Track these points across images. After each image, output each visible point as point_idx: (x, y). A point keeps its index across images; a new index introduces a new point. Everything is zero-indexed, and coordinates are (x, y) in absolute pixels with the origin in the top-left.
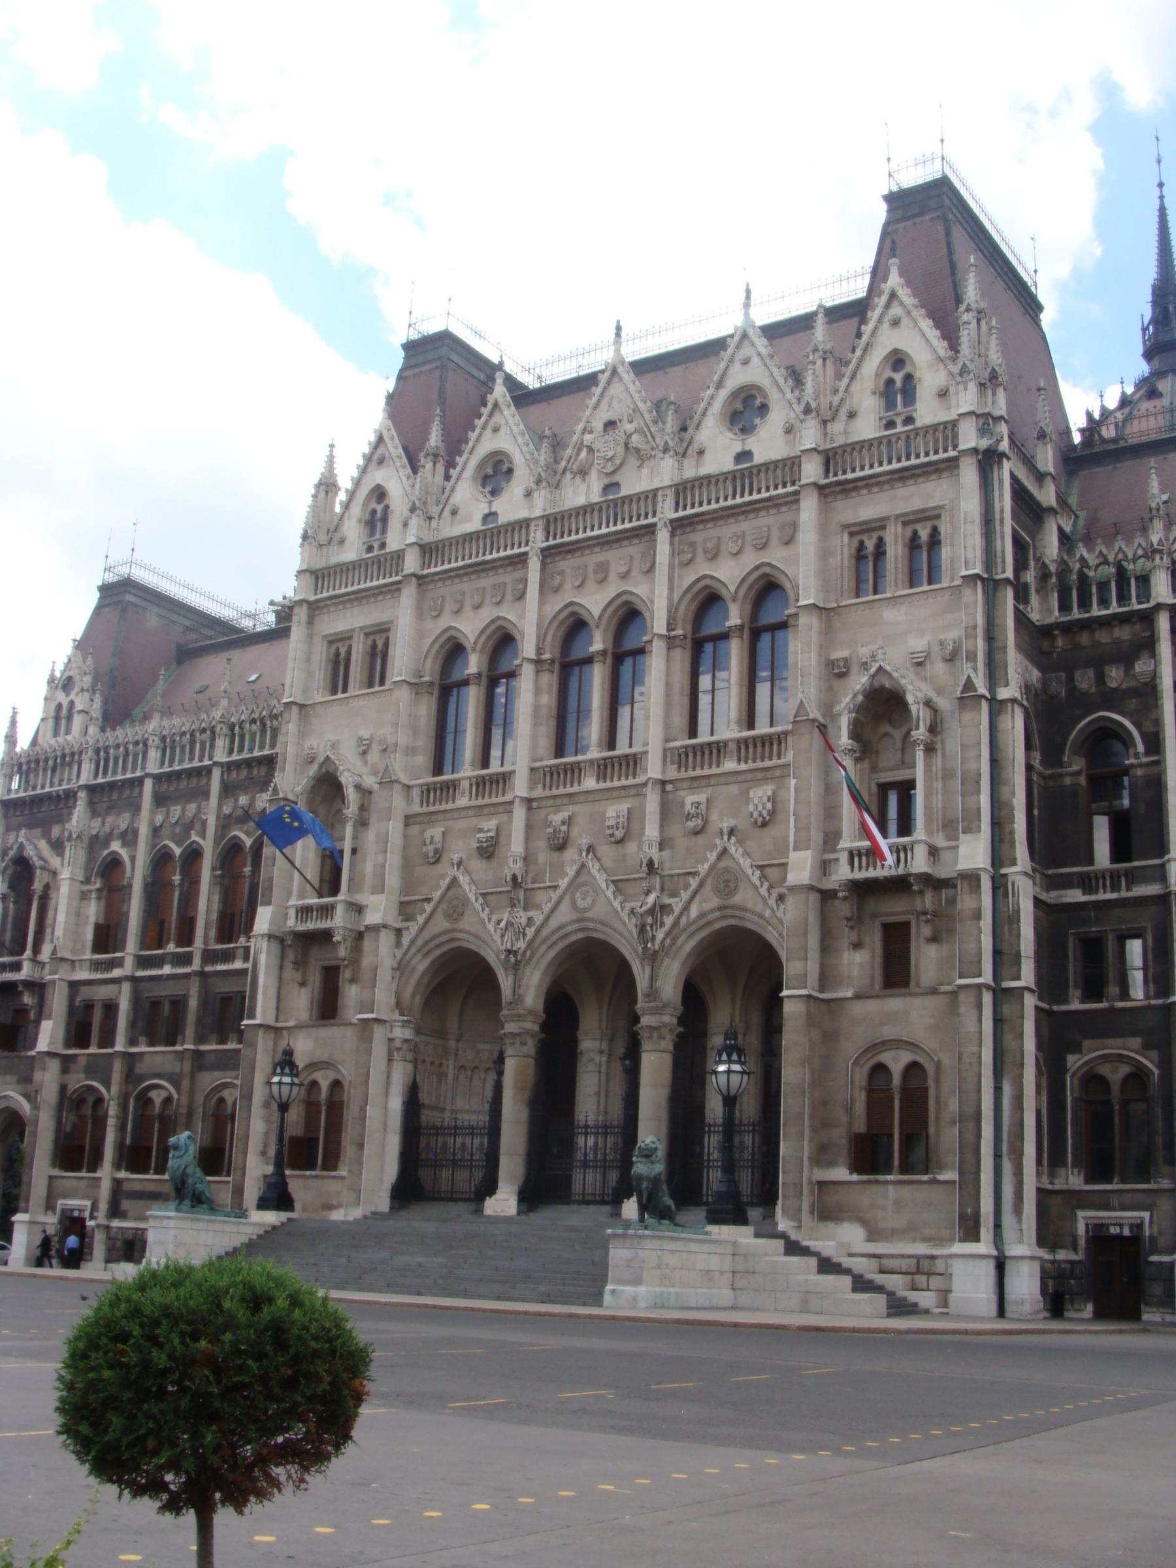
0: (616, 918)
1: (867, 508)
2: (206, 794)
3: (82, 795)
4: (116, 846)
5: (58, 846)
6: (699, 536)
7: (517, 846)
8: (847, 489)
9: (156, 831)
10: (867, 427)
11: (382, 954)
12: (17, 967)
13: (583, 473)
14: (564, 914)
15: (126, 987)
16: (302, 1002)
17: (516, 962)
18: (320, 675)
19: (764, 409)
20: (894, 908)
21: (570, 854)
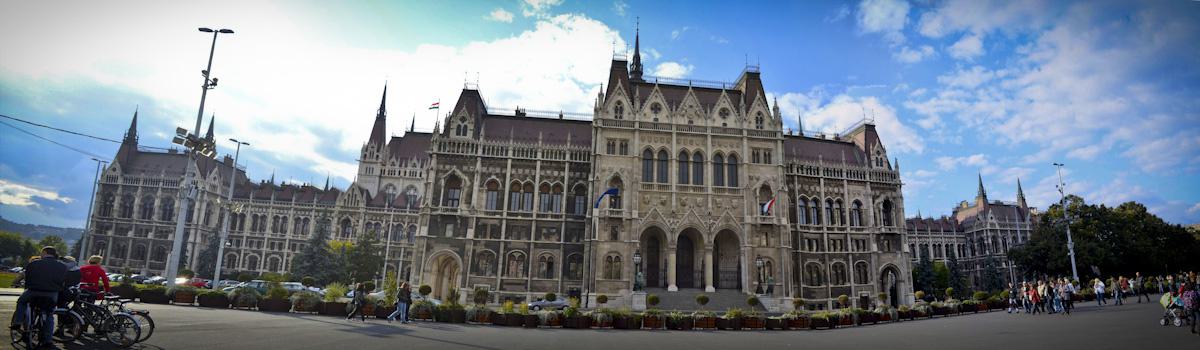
0: (702, 224)
1: (757, 145)
2: (535, 168)
3: (479, 159)
4: (494, 177)
5: (472, 175)
6: (717, 140)
7: (674, 204)
8: (753, 139)
9: (511, 175)
10: (753, 126)
11: (635, 226)
12: (456, 211)
13: (683, 116)
14: (687, 221)
15: (504, 222)
16: (606, 235)
17: (673, 231)
18: (605, 148)
19: (727, 114)
20: (765, 229)
21: (687, 207)
